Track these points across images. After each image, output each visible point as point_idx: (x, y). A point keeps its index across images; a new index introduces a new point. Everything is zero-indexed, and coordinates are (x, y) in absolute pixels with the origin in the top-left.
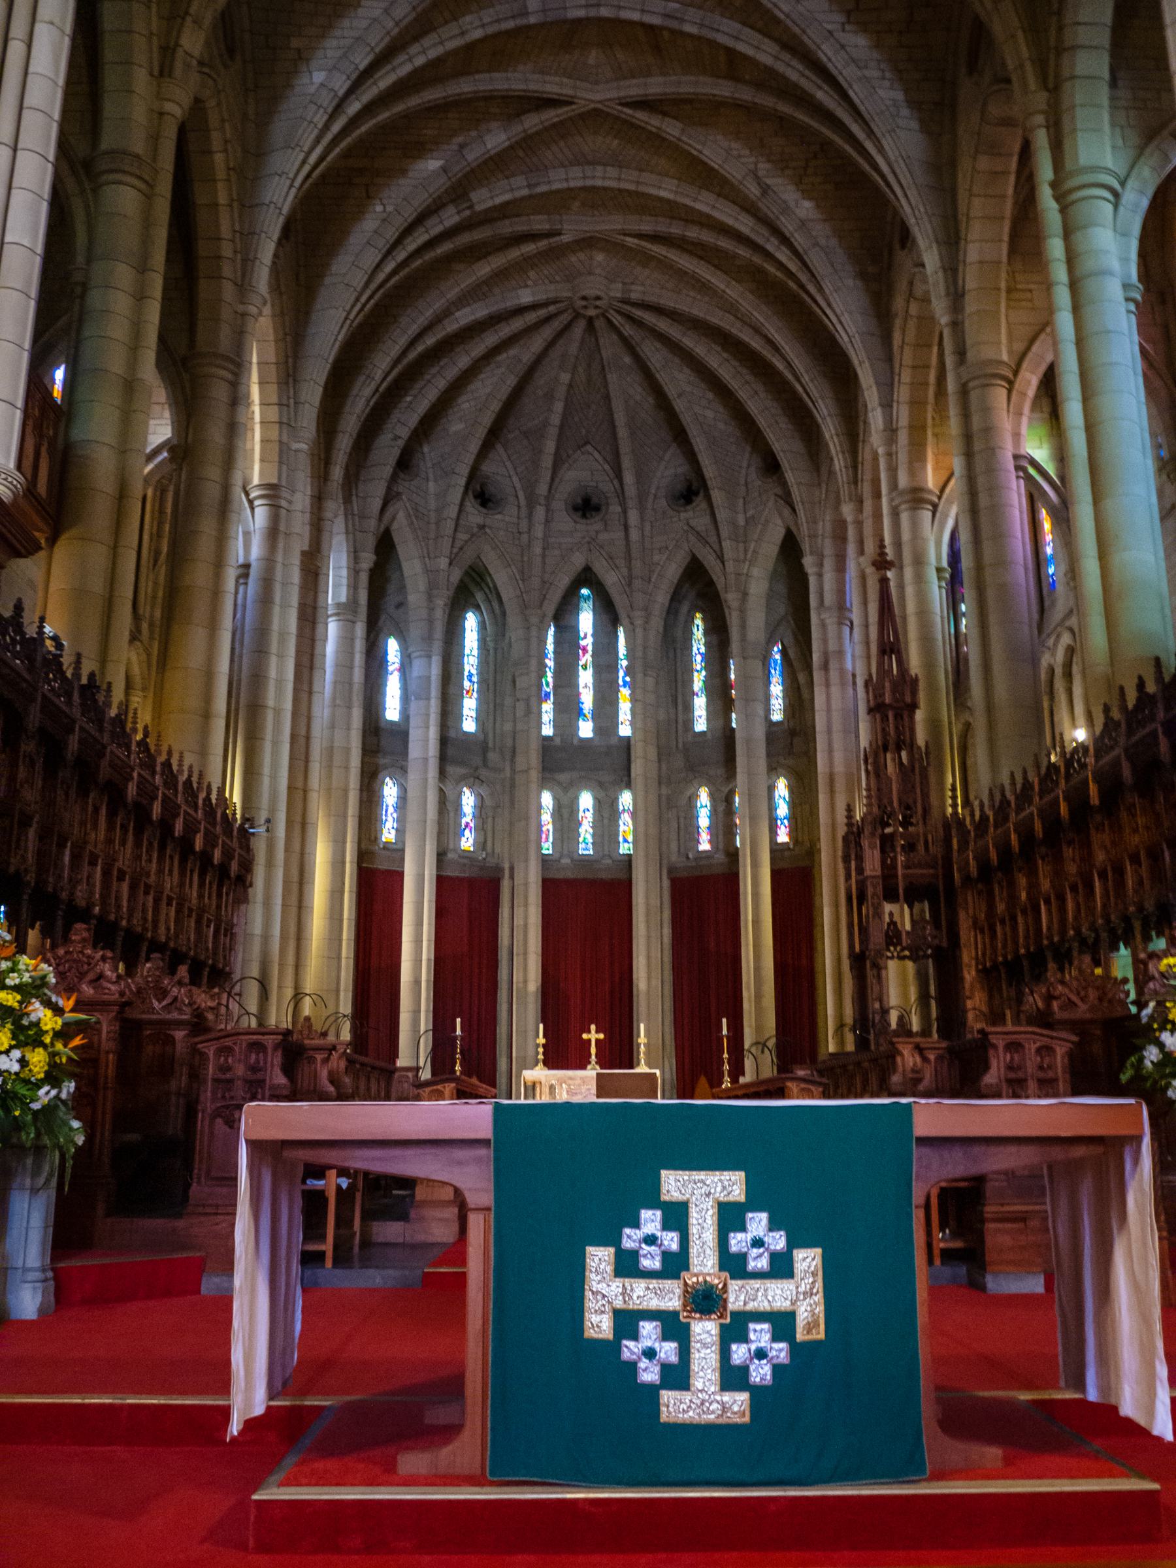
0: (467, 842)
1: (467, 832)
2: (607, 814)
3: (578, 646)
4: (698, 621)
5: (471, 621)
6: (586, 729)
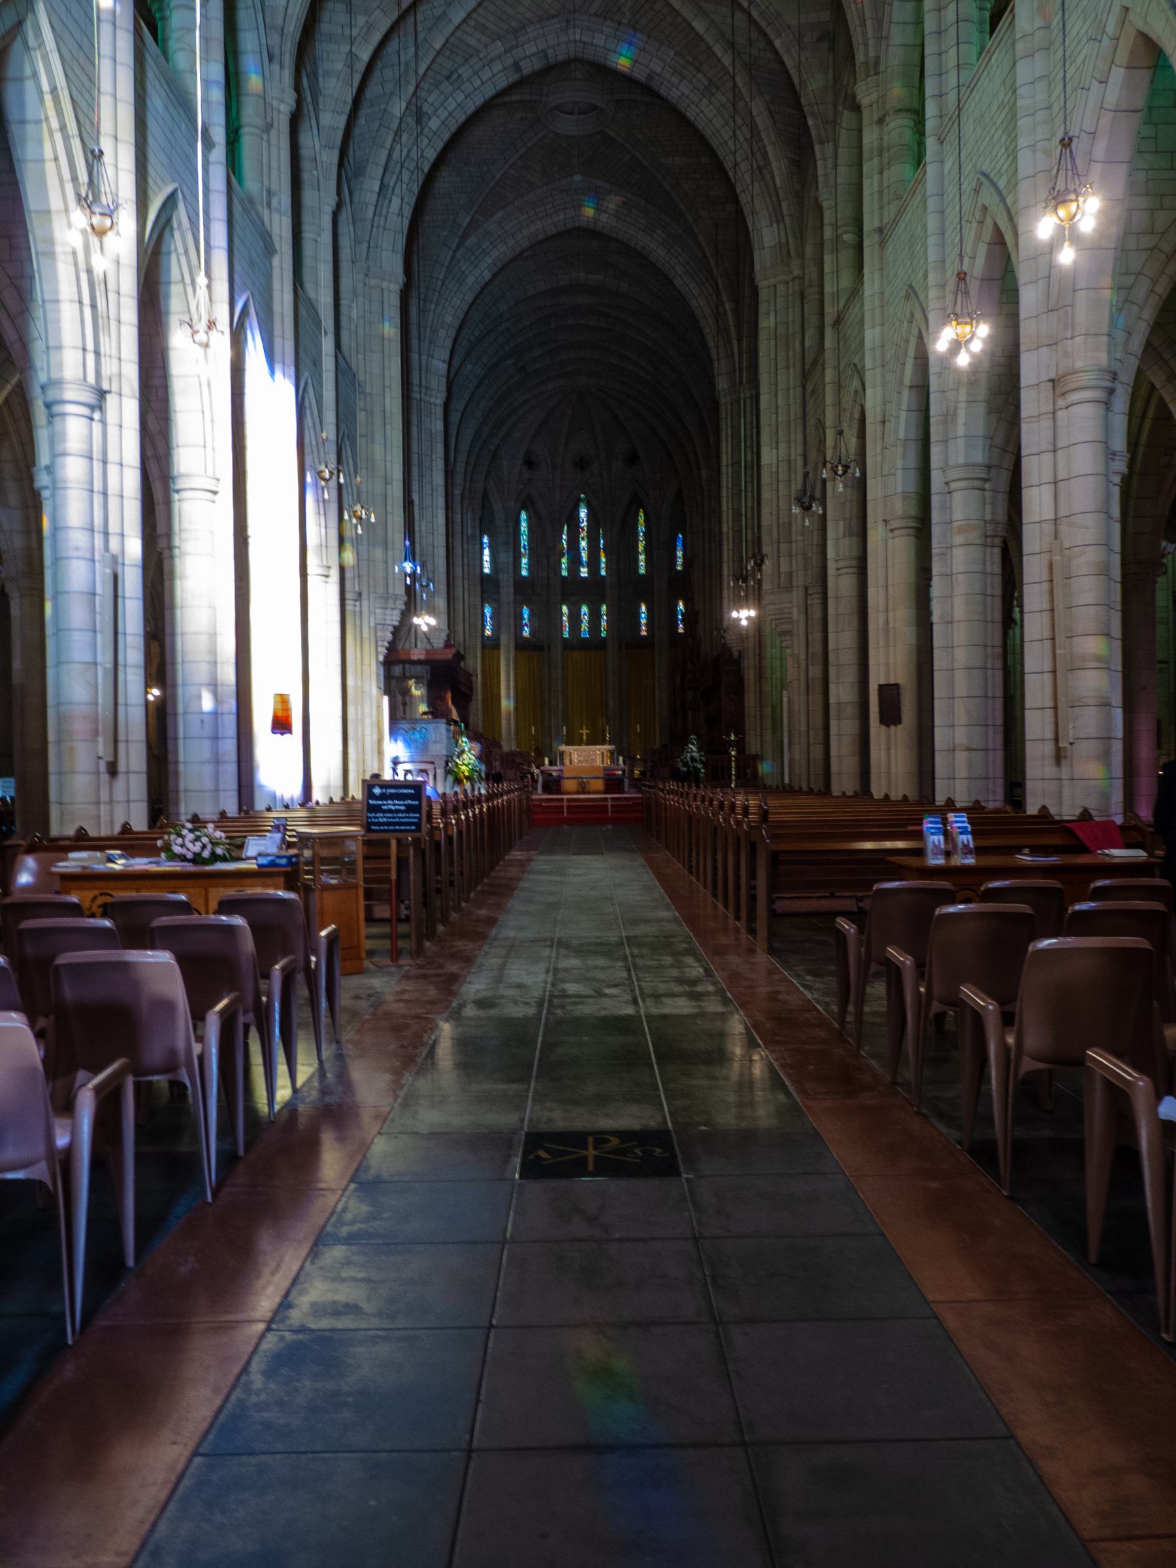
0: (526, 632)
1: (526, 628)
2: (595, 617)
3: (579, 527)
4: (641, 514)
5: (524, 516)
6: (584, 572)
